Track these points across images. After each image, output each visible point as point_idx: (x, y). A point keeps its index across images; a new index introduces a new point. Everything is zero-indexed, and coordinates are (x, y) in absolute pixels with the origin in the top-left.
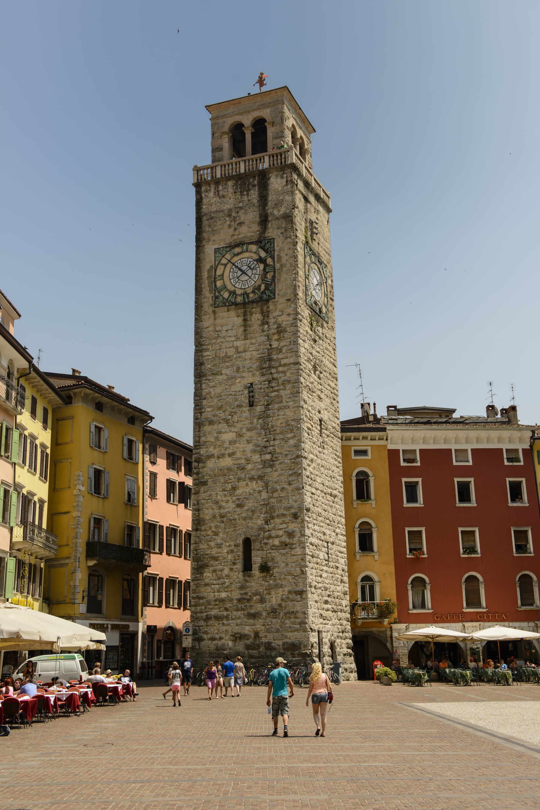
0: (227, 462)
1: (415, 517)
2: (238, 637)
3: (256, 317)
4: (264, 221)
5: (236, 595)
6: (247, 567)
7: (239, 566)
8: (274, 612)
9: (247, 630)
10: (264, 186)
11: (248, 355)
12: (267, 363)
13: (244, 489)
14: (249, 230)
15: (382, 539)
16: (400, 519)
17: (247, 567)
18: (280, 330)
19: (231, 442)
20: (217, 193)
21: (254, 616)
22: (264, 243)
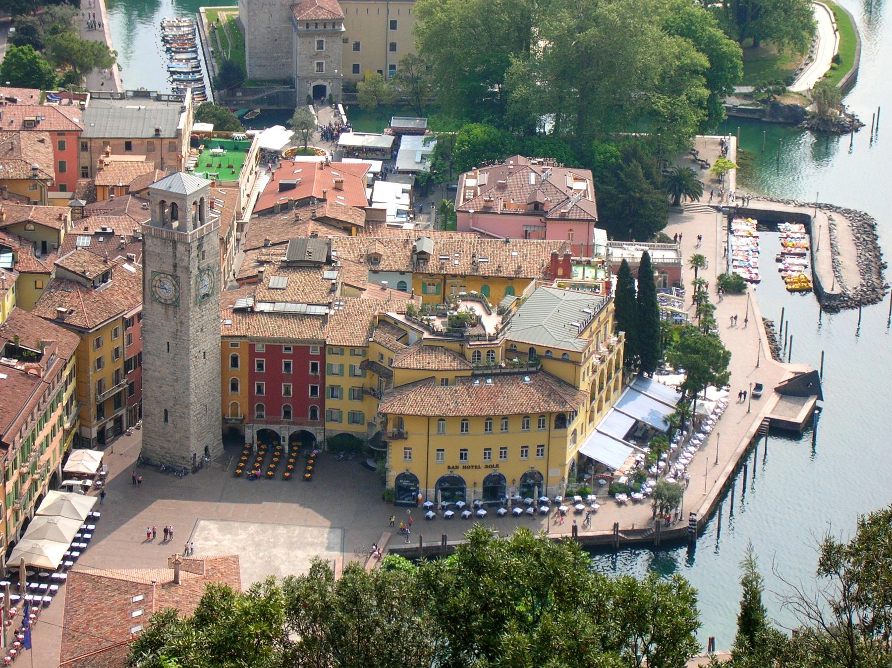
0: (157, 374)
1: (260, 377)
2: (162, 448)
3: (171, 312)
4: (175, 266)
5: (161, 431)
6: (166, 420)
7: (163, 420)
8: (176, 442)
9: (165, 446)
10: (175, 248)
11: (166, 329)
12: (175, 335)
13: (164, 388)
14: (168, 268)
15: (243, 386)
16: (252, 377)
17: (166, 420)
18: (181, 323)
19: (160, 366)
20: (152, 242)
21: (169, 441)
22: (175, 277)
